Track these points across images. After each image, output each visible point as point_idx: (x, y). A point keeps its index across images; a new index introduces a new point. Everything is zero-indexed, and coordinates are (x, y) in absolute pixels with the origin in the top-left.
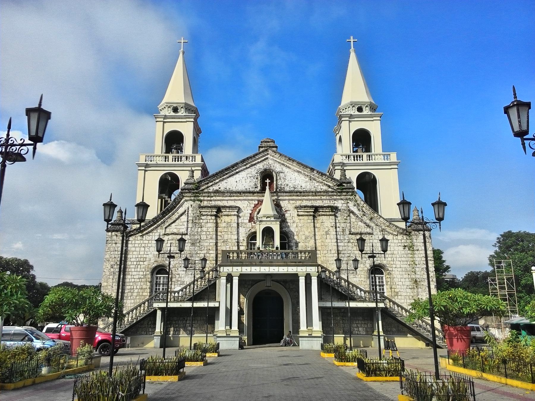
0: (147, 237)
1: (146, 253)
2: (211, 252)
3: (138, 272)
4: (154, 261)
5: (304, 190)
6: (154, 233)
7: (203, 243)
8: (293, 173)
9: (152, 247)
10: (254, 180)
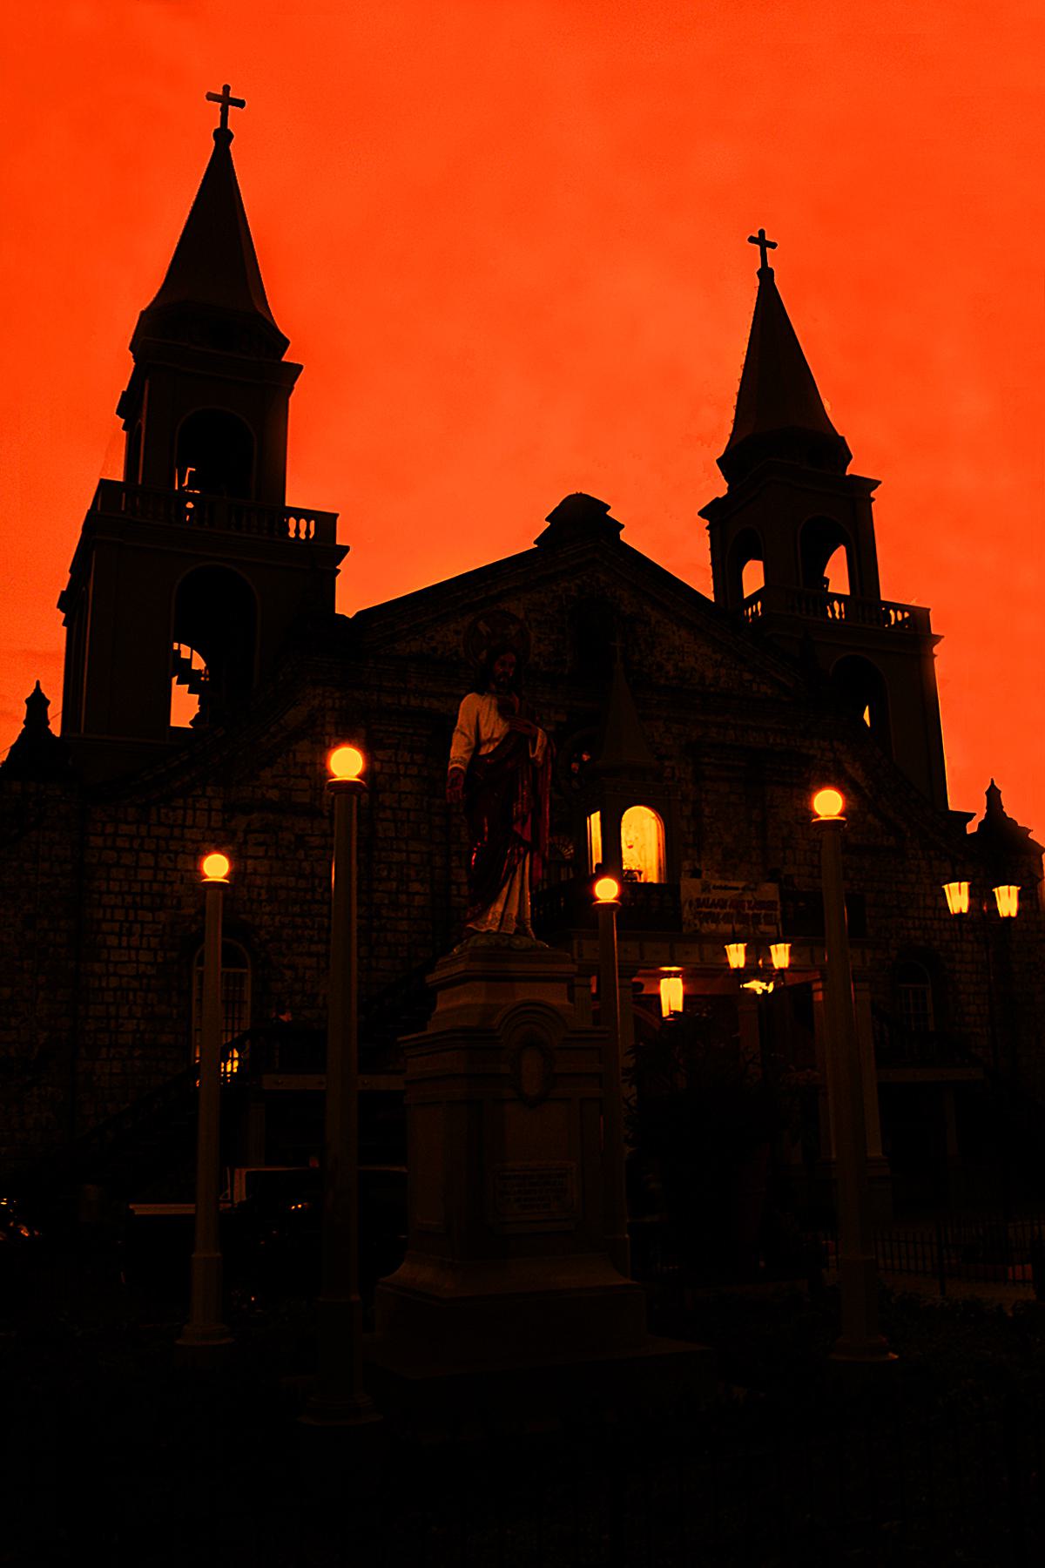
0: (163, 811)
1: (161, 876)
2: (415, 887)
3: (133, 952)
4: (193, 911)
5: (712, 689)
6: (190, 800)
7: (383, 854)
8: (675, 628)
9: (183, 852)
10: (553, 637)
